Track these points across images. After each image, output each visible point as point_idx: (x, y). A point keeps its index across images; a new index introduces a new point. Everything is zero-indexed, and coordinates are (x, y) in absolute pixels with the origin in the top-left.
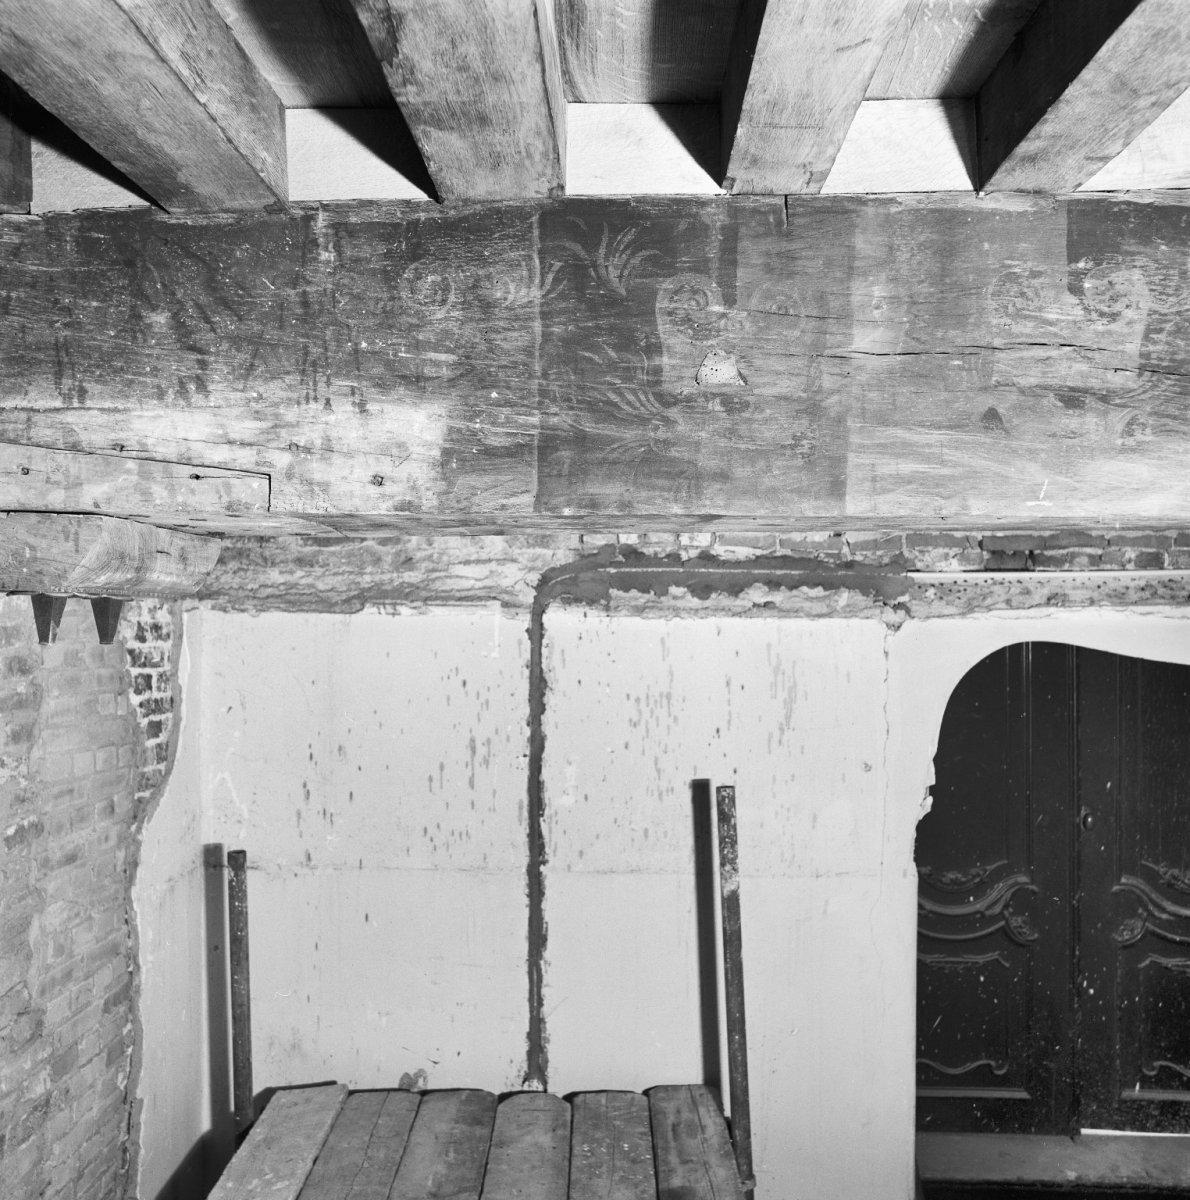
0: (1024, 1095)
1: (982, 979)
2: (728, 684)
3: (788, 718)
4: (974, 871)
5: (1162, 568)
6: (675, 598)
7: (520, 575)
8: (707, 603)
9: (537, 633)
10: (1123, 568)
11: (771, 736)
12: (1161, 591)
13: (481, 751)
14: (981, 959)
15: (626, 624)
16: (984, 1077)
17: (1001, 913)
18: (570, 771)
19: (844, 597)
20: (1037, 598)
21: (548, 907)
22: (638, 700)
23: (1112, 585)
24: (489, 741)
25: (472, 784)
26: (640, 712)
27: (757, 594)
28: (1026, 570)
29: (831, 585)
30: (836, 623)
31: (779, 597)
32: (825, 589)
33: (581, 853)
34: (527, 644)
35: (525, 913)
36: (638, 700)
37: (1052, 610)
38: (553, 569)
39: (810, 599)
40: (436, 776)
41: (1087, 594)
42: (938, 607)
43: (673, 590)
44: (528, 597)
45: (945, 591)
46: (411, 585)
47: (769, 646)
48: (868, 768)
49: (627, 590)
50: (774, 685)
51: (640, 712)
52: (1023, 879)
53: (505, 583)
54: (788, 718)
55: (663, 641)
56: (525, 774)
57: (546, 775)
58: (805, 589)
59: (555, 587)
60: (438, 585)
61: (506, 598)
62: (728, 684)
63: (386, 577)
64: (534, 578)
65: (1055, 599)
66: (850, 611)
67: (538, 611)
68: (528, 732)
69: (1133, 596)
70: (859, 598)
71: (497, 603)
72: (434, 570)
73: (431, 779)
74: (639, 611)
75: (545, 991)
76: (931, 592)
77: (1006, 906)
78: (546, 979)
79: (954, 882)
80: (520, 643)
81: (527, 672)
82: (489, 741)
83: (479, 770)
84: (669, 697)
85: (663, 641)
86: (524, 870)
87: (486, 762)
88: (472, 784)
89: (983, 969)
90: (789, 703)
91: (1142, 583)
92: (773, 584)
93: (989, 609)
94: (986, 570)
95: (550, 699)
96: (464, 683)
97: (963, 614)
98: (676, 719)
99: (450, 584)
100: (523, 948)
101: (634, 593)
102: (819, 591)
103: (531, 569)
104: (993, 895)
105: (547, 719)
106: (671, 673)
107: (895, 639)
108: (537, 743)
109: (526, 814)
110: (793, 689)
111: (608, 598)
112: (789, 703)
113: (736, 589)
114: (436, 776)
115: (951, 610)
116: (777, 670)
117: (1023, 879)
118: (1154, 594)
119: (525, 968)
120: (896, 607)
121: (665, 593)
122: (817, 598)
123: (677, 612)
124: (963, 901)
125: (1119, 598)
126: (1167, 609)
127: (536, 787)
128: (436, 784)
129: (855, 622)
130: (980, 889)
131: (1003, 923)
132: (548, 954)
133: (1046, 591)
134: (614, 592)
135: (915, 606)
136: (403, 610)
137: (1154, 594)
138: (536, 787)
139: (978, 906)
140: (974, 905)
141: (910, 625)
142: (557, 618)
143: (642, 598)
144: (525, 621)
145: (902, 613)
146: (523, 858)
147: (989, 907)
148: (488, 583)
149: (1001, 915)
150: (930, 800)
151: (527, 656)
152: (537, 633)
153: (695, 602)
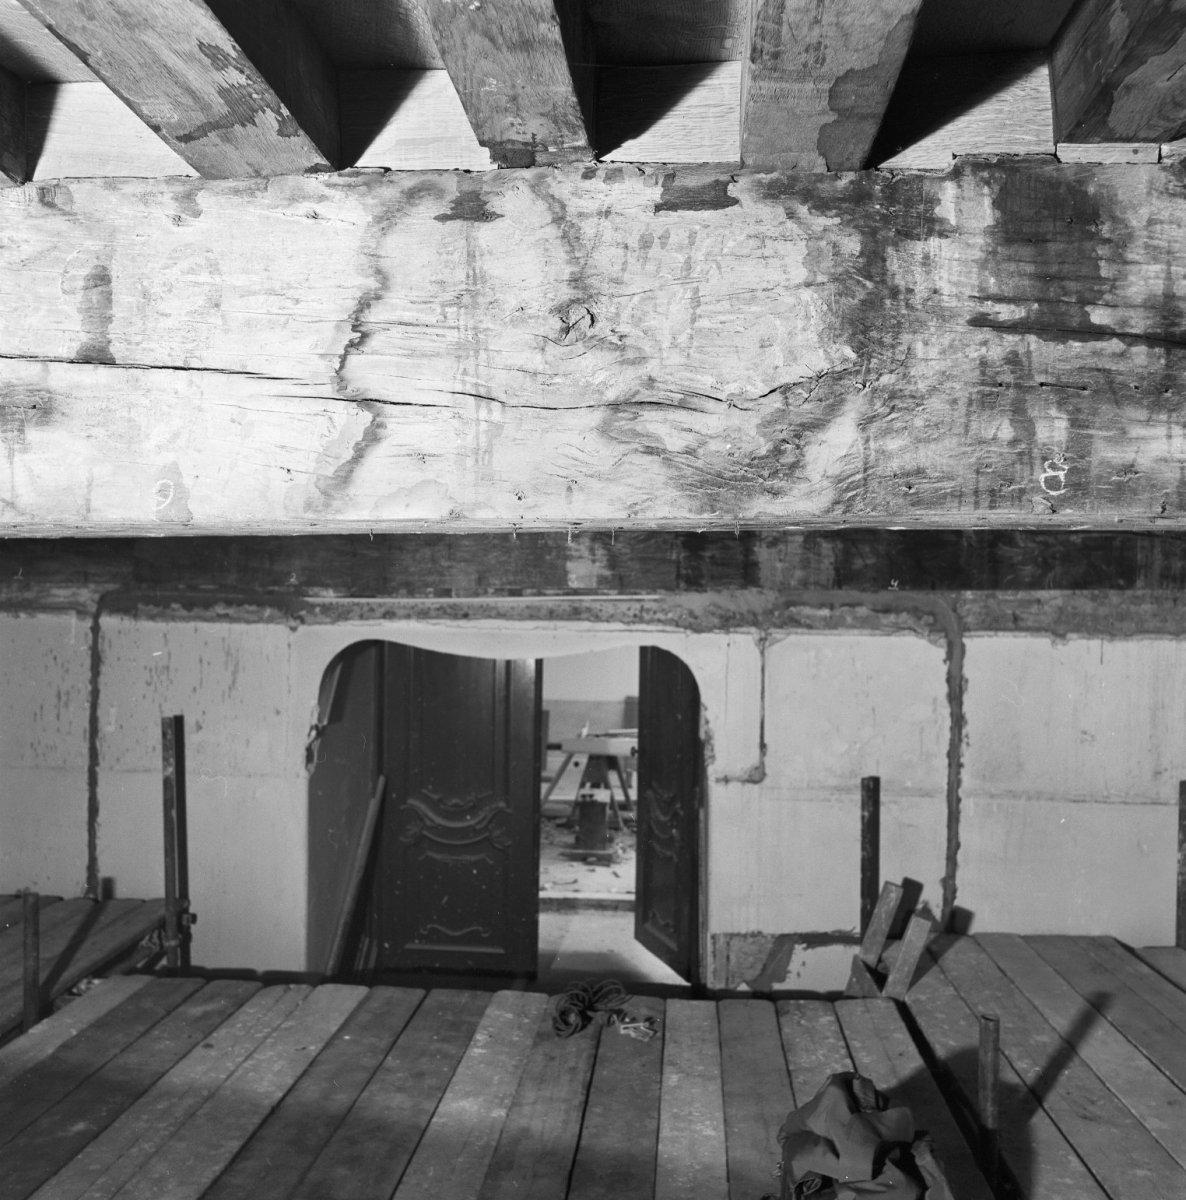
0: (502, 951)
1: (475, 872)
2: (201, 661)
3: (234, 682)
4: (469, 798)
5: (451, 597)
6: (174, 610)
7: (89, 595)
8: (192, 614)
9: (96, 629)
10: (427, 597)
11: (224, 692)
12: (449, 611)
13: (64, 698)
14: (473, 858)
15: (146, 625)
16: (473, 938)
17: (486, 827)
18: (113, 711)
19: (268, 612)
20: (378, 614)
21: (100, 791)
22: (151, 670)
23: (421, 606)
24: (68, 693)
25: (58, 717)
26: (152, 677)
27: (220, 609)
28: (373, 597)
29: (261, 604)
30: (261, 626)
31: (231, 611)
32: (258, 605)
33: (118, 760)
34: (90, 635)
35: (86, 795)
36: (151, 670)
37: (382, 621)
38: (108, 592)
39: (248, 612)
40: (38, 712)
41: (406, 612)
42: (321, 618)
43: (174, 606)
44: (93, 608)
45: (326, 609)
46: (27, 600)
47: (223, 639)
48: (278, 713)
49: (147, 604)
50: (226, 663)
51: (152, 677)
52: (502, 804)
53: (82, 599)
54: (234, 682)
55: (165, 635)
56: (88, 713)
57: (100, 713)
58: (247, 606)
59: (110, 604)
60: (43, 601)
61: (81, 608)
62: (201, 661)
63: (14, 595)
64: (97, 597)
65: (389, 615)
66: (270, 620)
67: (96, 617)
68: (90, 688)
69: (433, 613)
70: (276, 612)
71: (73, 613)
72: (41, 592)
73: (36, 714)
74: (152, 618)
75: (98, 842)
76: (317, 610)
77: (490, 822)
78: (99, 834)
79: (456, 805)
80: (86, 635)
81: (90, 652)
82: (68, 693)
83: (63, 710)
84: (168, 668)
85: (165, 635)
86: (86, 768)
87: (66, 705)
88: (58, 717)
89: (475, 864)
90: (235, 673)
91: (438, 606)
92: (229, 603)
93: (346, 619)
94: (352, 596)
95: (104, 669)
96: (55, 658)
97: (333, 623)
98: (171, 683)
99: (50, 600)
100: (84, 815)
101: (151, 607)
102: (253, 608)
103: (96, 592)
104: (482, 815)
105: (102, 679)
106: (169, 654)
107: (293, 637)
108: (95, 694)
109: (88, 735)
110: (237, 665)
111: (137, 609)
112: (235, 673)
113: (207, 605)
114: (38, 712)
115: (328, 620)
116: (228, 654)
117: (502, 804)
118: (445, 612)
119: (85, 827)
120: (295, 619)
121: (167, 606)
122: (252, 612)
123: (173, 619)
124: (462, 818)
125: (424, 614)
126: (448, 622)
127: (94, 721)
128: (38, 716)
129: (272, 626)
130: (473, 810)
131: (487, 834)
132: (100, 819)
133: (383, 610)
134: (140, 606)
135: (309, 618)
136: (23, 615)
137: (445, 612)
138: (94, 721)
139: (472, 822)
140: (470, 821)
141: (302, 629)
142: (108, 622)
143: (155, 610)
144: (89, 623)
145: (298, 622)
146: (85, 762)
147: (479, 823)
148: (72, 599)
149: (486, 828)
150: (314, 733)
151: (90, 642)
152: (96, 629)
153: (184, 613)
